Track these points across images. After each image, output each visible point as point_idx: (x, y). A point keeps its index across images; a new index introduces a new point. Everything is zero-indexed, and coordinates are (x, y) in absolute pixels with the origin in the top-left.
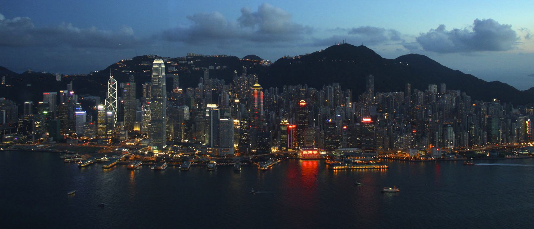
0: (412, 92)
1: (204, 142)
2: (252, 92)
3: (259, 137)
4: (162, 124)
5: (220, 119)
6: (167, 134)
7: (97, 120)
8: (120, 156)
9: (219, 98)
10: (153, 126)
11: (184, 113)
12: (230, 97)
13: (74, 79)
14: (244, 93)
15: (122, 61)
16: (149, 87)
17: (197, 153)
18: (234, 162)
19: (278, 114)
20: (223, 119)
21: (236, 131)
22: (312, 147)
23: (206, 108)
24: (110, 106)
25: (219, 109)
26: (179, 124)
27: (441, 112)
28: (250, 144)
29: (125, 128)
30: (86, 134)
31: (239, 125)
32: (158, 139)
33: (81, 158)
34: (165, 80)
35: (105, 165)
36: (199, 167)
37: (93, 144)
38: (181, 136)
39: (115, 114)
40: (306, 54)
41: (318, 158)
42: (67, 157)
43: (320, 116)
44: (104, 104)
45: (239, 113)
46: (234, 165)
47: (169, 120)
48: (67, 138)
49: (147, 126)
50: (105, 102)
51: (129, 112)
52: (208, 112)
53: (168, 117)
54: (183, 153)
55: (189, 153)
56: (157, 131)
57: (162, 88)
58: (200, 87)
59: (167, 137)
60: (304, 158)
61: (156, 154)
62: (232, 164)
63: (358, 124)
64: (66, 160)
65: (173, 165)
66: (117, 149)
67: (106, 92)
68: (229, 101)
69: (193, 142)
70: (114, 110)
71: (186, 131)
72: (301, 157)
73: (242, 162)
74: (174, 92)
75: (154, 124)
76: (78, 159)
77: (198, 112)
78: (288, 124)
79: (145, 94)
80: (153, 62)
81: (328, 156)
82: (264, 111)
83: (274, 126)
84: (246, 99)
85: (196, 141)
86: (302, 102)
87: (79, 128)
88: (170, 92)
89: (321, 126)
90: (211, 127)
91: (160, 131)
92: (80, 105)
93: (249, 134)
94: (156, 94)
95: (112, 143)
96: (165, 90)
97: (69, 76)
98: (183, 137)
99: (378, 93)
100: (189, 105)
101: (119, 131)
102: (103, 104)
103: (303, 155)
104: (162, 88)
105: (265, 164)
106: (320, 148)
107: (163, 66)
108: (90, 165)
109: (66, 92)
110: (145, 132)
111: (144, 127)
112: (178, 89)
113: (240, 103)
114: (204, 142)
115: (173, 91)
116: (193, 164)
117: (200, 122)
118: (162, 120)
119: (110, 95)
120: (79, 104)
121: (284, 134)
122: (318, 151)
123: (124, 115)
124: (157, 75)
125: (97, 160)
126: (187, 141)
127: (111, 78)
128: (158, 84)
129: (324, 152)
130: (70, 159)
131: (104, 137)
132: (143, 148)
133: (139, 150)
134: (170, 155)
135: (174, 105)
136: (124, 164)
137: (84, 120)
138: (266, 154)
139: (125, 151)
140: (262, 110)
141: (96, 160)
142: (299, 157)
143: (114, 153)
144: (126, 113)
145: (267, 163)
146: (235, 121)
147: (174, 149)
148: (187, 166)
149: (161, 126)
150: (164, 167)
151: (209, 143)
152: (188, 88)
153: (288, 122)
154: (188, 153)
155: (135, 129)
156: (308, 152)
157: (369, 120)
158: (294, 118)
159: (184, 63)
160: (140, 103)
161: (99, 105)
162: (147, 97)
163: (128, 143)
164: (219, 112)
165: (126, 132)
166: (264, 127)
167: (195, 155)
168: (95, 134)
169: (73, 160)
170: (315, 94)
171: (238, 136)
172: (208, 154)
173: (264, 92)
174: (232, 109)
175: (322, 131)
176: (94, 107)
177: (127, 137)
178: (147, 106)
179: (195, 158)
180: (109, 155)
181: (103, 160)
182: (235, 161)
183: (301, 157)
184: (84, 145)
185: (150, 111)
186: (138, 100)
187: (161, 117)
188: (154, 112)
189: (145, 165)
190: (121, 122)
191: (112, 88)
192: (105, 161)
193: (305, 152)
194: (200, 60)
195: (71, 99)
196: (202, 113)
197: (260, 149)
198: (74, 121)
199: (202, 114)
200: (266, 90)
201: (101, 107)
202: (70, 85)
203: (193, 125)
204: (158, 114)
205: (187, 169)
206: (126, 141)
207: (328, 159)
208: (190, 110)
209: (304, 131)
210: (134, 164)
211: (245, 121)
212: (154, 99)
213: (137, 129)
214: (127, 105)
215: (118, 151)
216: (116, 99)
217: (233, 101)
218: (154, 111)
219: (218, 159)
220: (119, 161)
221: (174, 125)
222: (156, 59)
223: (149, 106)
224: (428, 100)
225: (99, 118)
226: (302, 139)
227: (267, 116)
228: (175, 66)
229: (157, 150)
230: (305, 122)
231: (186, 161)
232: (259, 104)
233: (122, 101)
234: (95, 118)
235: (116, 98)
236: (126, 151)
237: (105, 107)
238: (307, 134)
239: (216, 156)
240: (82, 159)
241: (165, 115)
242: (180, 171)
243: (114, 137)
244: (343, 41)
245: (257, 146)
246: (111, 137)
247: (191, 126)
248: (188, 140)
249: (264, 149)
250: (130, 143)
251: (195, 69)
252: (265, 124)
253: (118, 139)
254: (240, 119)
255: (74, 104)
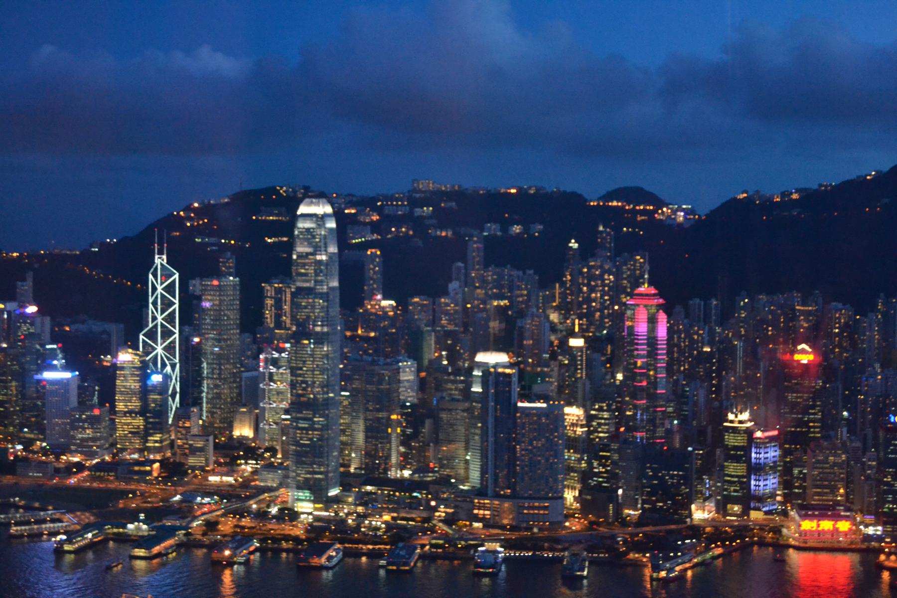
1: (465, 480)
2: (629, 313)
3: (649, 468)
4: (326, 417)
5: (520, 404)
6: (341, 451)
7: (115, 401)
8: (189, 519)
9: (516, 332)
10: (297, 423)
11: (399, 381)
12: (553, 328)
13: (36, 266)
14: (602, 317)
15: (196, 205)
16: (285, 291)
17: (440, 516)
18: (563, 550)
20: (527, 405)
21: (573, 443)
22: (834, 509)
23: (474, 365)
24: (156, 355)
25: (517, 368)
26: (382, 418)
28: (620, 492)
29: (206, 431)
30: (79, 446)
31: (582, 426)
32: (311, 464)
33: (64, 524)
34: (335, 269)
35: (140, 546)
36: (447, 562)
37: (101, 479)
38: (388, 457)
39: (174, 381)
40: (820, 185)
41: (853, 546)
42: (18, 519)
43: (864, 402)
44: (138, 349)
45: (584, 384)
46: (563, 561)
47: (350, 404)
48: (16, 456)
49: (276, 423)
50: (141, 341)
51: (220, 374)
52: (480, 380)
53: (347, 394)
54: (395, 515)
55: (414, 516)
56: (311, 439)
57: (325, 296)
58: (452, 294)
59: (343, 460)
60: (806, 543)
61: (306, 516)
62: (556, 554)
64: (14, 530)
65: (358, 554)
66: (178, 498)
67: (144, 309)
68: (552, 343)
69: (429, 479)
70: (168, 369)
71: (405, 441)
72: (794, 539)
73: (590, 550)
74: (366, 311)
75: (299, 415)
76: (54, 527)
77: (446, 377)
78: (749, 424)
79: (271, 316)
80: (297, 208)
81: (890, 543)
82: (668, 382)
84: (610, 339)
85: (437, 475)
86: (803, 352)
87: (57, 424)
88: (354, 310)
89: (865, 435)
90: (487, 428)
91: (319, 440)
92: (58, 351)
93: (616, 457)
94: (308, 317)
95: (163, 475)
96: (338, 305)
97: (21, 255)
98: (394, 460)
100: (415, 353)
101: (187, 439)
102: (133, 349)
103: (800, 536)
104: (328, 297)
105: (667, 559)
106: (862, 512)
107: (332, 224)
108: (91, 545)
109: (12, 306)
110: (269, 441)
111: (267, 427)
112: (380, 301)
113: (587, 349)
114: (465, 480)
115: (362, 305)
116: (426, 552)
117: (450, 410)
118: (327, 403)
119: (154, 318)
120: (55, 346)
121: (737, 459)
122: (854, 523)
123: (200, 384)
124: (311, 254)
125: (115, 530)
126: (407, 473)
127: (160, 260)
128: (312, 284)
129: (874, 525)
130: (27, 527)
131: (136, 456)
132: (264, 492)
133: (251, 502)
134: (350, 521)
135: (366, 352)
136: (199, 545)
137: (74, 400)
138: (673, 527)
139: (206, 504)
140: (662, 375)
141: (110, 531)
142: (787, 540)
143: (168, 510)
144: (208, 378)
145: (676, 556)
146: (567, 410)
147: (364, 499)
148: (407, 556)
149: (325, 422)
150: (330, 558)
151: (481, 484)
152: (413, 297)
153: (750, 421)
154: (412, 513)
155: (237, 433)
156: (818, 526)
159: (400, 213)
160: (255, 347)
161: (123, 349)
162: (279, 324)
163: (213, 479)
164: (515, 379)
165: (208, 440)
166: (669, 432)
167: (434, 522)
168: (107, 446)
169: (38, 528)
170: (846, 324)
171: (579, 460)
172: (477, 519)
174: (559, 370)
176: (105, 356)
177: (213, 459)
178: (276, 355)
179: (433, 530)
180: (153, 516)
181: (135, 533)
182: (567, 545)
183: (794, 539)
184: (73, 481)
185: (288, 371)
186: (247, 335)
187: (324, 393)
188: (300, 375)
189: (272, 550)
190: (192, 409)
191: (162, 296)
192: (140, 534)
193: (808, 525)
194: (454, 204)
195: (29, 329)
196: (462, 382)
197: (654, 509)
198: (39, 403)
199: (461, 386)
200: (678, 309)
201: (125, 357)
202: (25, 283)
203: (428, 423)
204: (314, 382)
205: (407, 568)
206: (208, 471)
207: (889, 555)
208: (419, 370)
209: (805, 452)
210: (234, 545)
211: (604, 411)
212: (302, 333)
213: (243, 430)
214: (212, 353)
215: (181, 502)
216: (175, 333)
217: (564, 343)
218: (301, 372)
219: (511, 539)
220: (185, 535)
221: (366, 420)
222: (307, 200)
223: (283, 355)
225: (122, 393)
226: (798, 478)
227: (678, 396)
228: (372, 223)
229: (309, 501)
230: (810, 421)
231: (402, 539)
232: (652, 352)
233: (196, 340)
234: (108, 396)
235: (175, 327)
236: (209, 504)
237: (140, 356)
238: (818, 462)
239: (503, 527)
240: (66, 526)
241: (337, 388)
242: (382, 572)
243: (168, 459)
245: (644, 498)
246: (158, 457)
247: (423, 424)
248: (411, 472)
249: (669, 509)
250: (222, 475)
251: (438, 233)
252: (672, 423)
253: (183, 464)
254: (588, 403)
255: (38, 347)
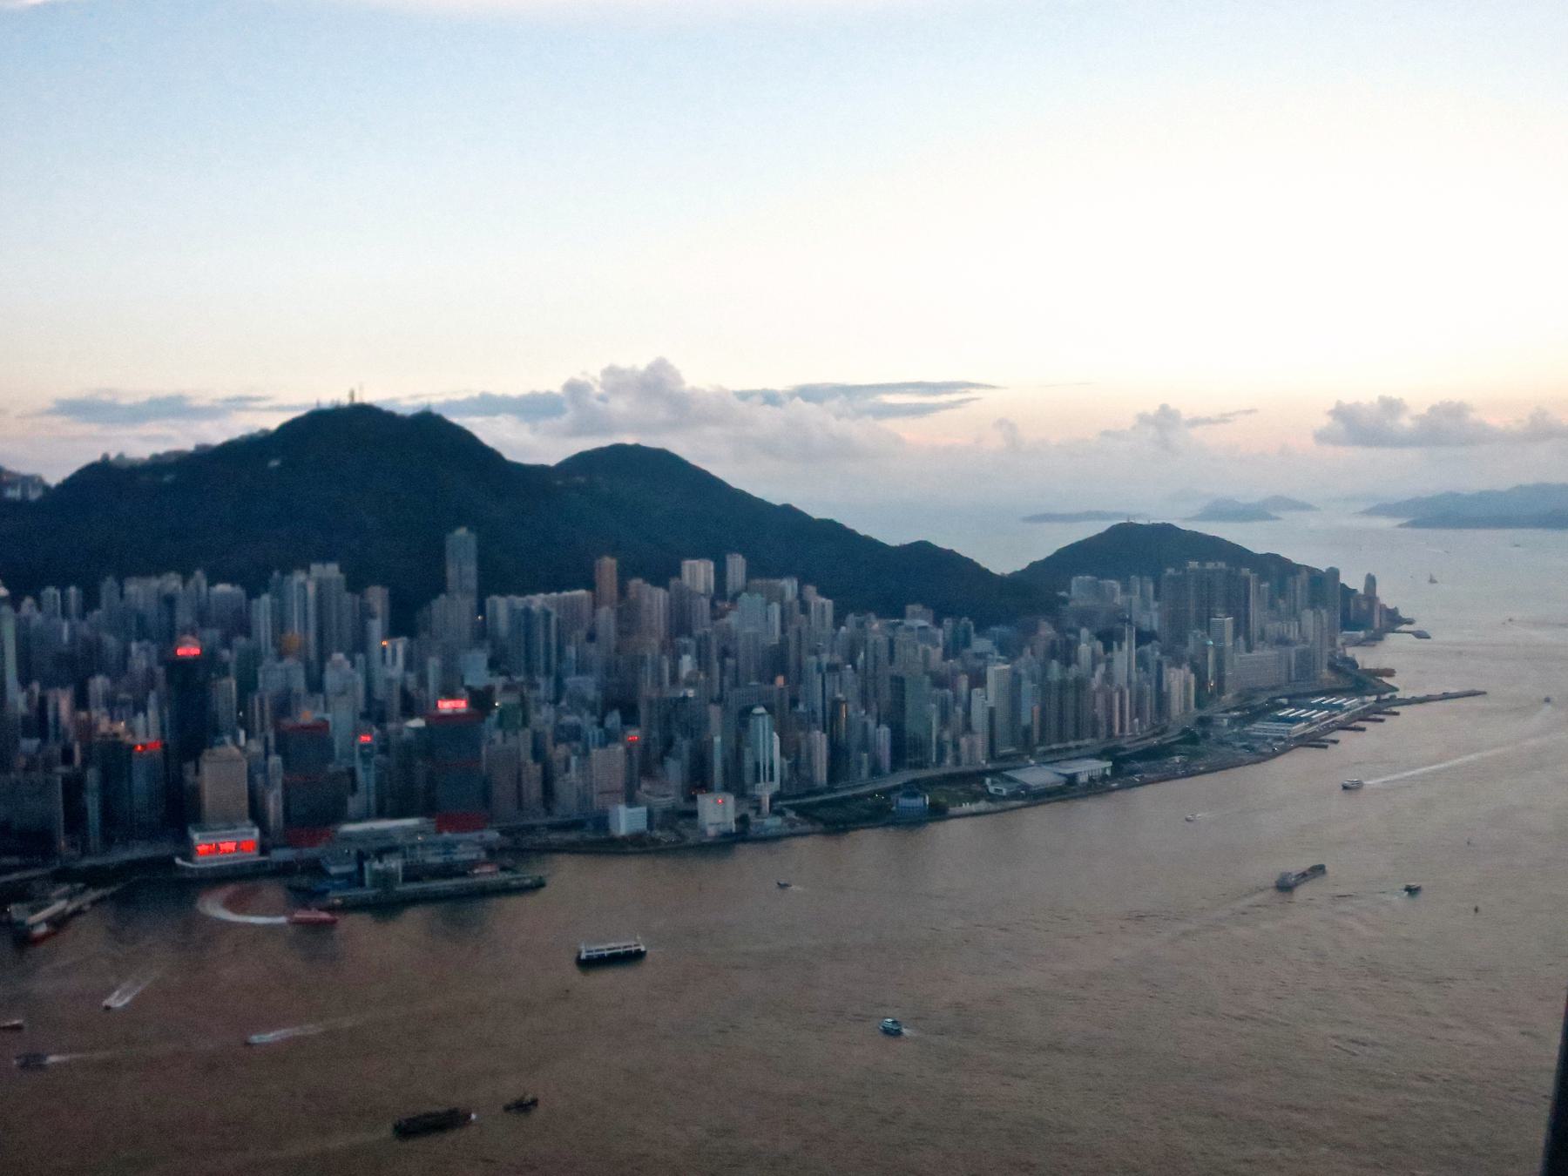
0: (623, 591)
19: (81, 701)
27: (730, 662)
63: (417, 723)
83: (67, 756)
89: (267, 739)
99: (495, 598)
105: (34, 911)
157: (462, 705)
158: (152, 713)
173: (17, 608)
175: (275, 760)
200: (28, 601)
224: (680, 623)
244: (352, 395)
